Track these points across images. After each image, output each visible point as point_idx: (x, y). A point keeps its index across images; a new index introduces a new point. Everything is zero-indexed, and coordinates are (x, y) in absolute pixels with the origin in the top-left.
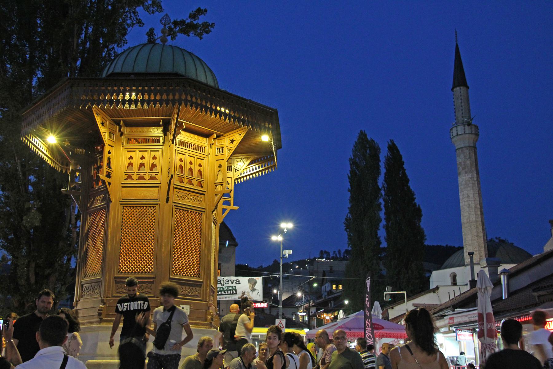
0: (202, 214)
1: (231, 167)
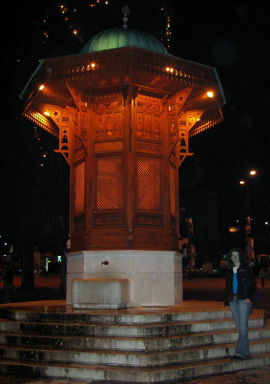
1: (186, 122)
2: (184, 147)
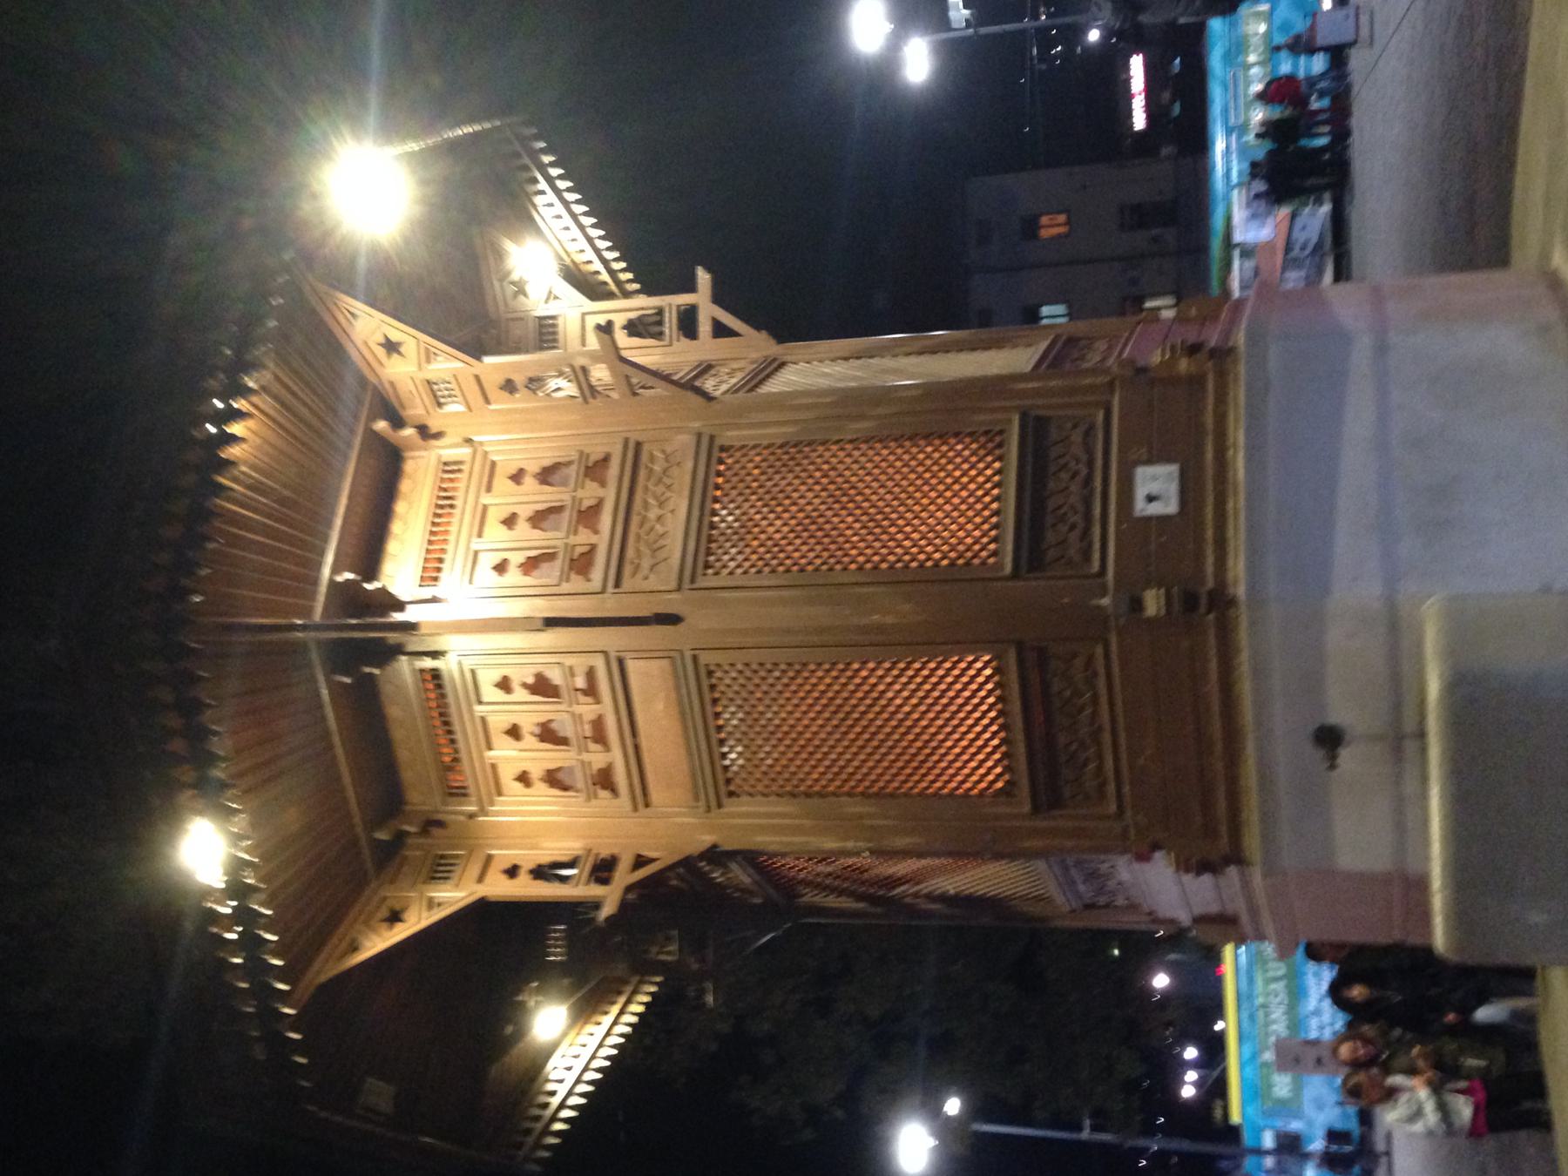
0: (723, 449)
2: (670, 323)
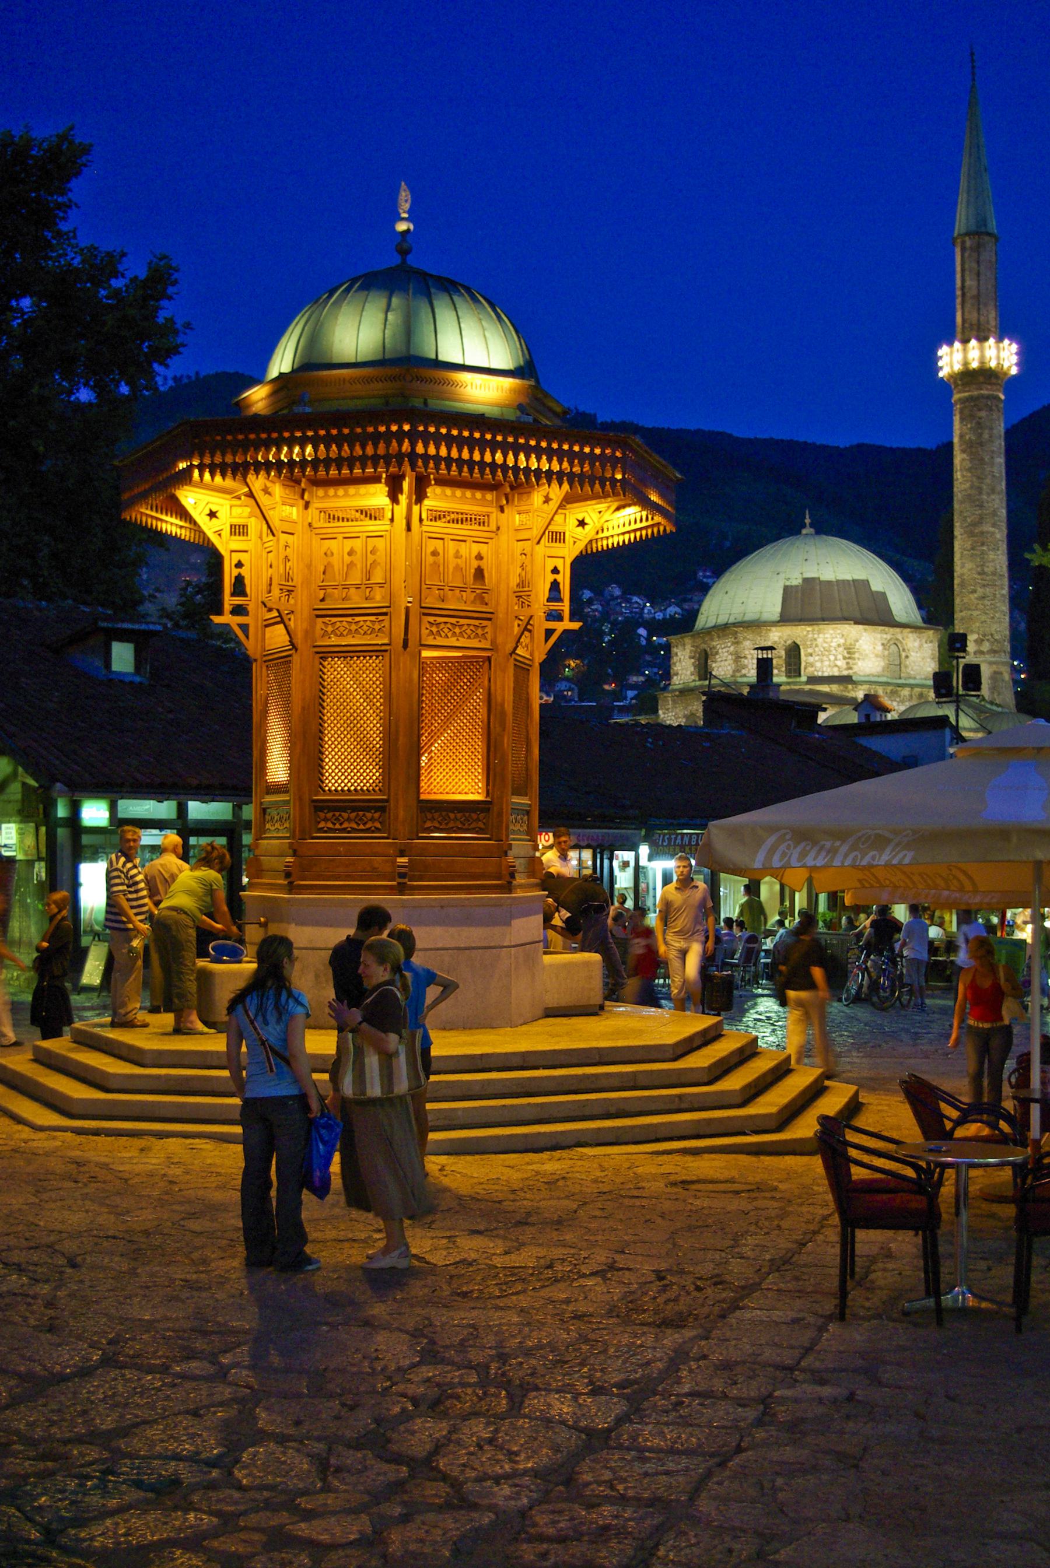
2: (555, 606)
